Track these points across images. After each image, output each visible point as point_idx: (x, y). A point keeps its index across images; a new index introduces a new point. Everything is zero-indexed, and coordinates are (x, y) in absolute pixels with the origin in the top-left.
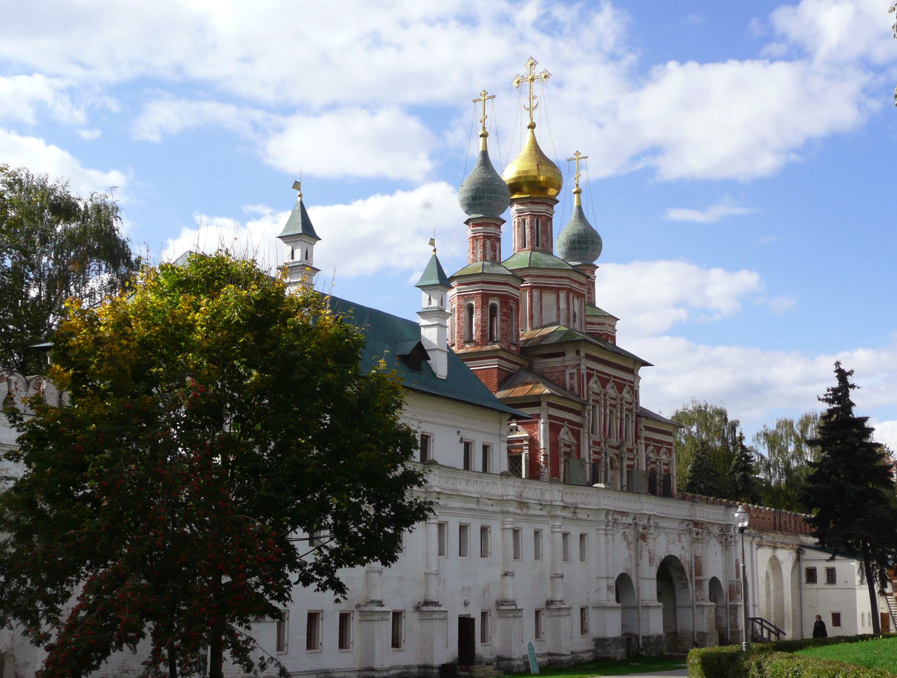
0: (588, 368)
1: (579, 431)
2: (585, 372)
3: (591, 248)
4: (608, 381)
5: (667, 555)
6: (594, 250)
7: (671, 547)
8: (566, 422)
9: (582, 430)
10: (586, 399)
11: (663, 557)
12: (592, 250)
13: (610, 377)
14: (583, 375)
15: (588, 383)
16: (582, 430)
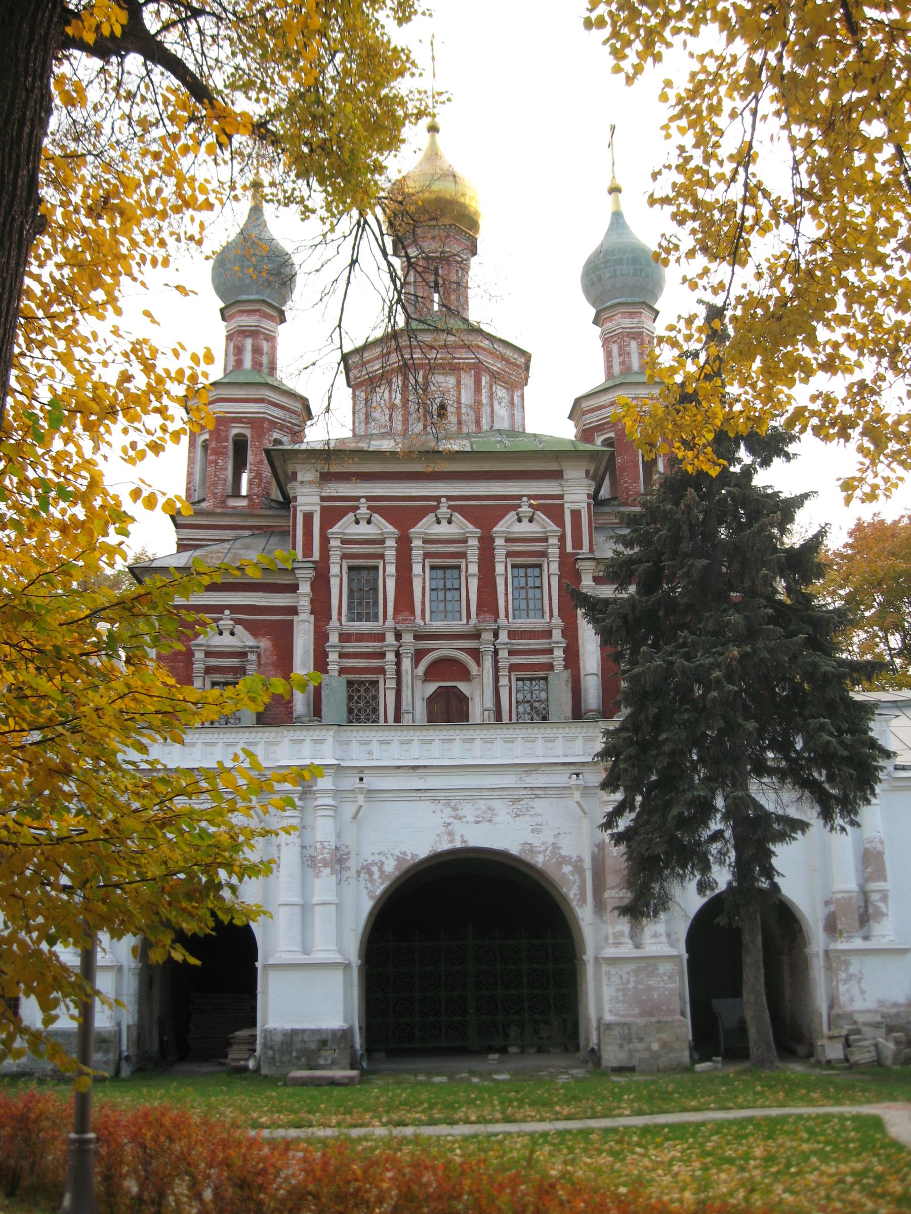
0: (323, 499)
1: (292, 621)
2: (318, 508)
3: (608, 275)
4: (434, 509)
5: (445, 846)
6: (616, 276)
7: (457, 827)
8: (227, 612)
9: (295, 618)
10: (316, 556)
11: (423, 852)
12: (611, 277)
13: (439, 502)
14: (308, 517)
15: (324, 527)
16: (296, 618)
